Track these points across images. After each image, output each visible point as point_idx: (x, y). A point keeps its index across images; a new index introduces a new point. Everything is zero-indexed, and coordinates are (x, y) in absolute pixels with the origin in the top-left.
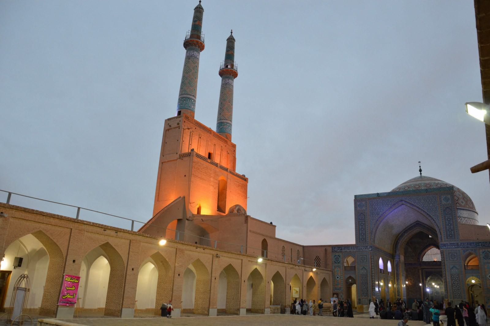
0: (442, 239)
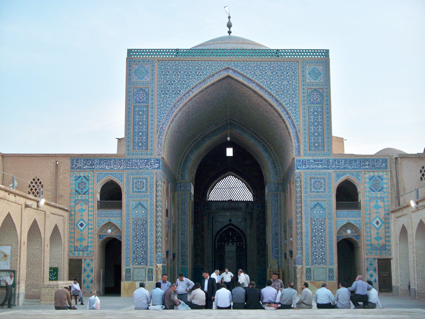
0: (299, 152)
